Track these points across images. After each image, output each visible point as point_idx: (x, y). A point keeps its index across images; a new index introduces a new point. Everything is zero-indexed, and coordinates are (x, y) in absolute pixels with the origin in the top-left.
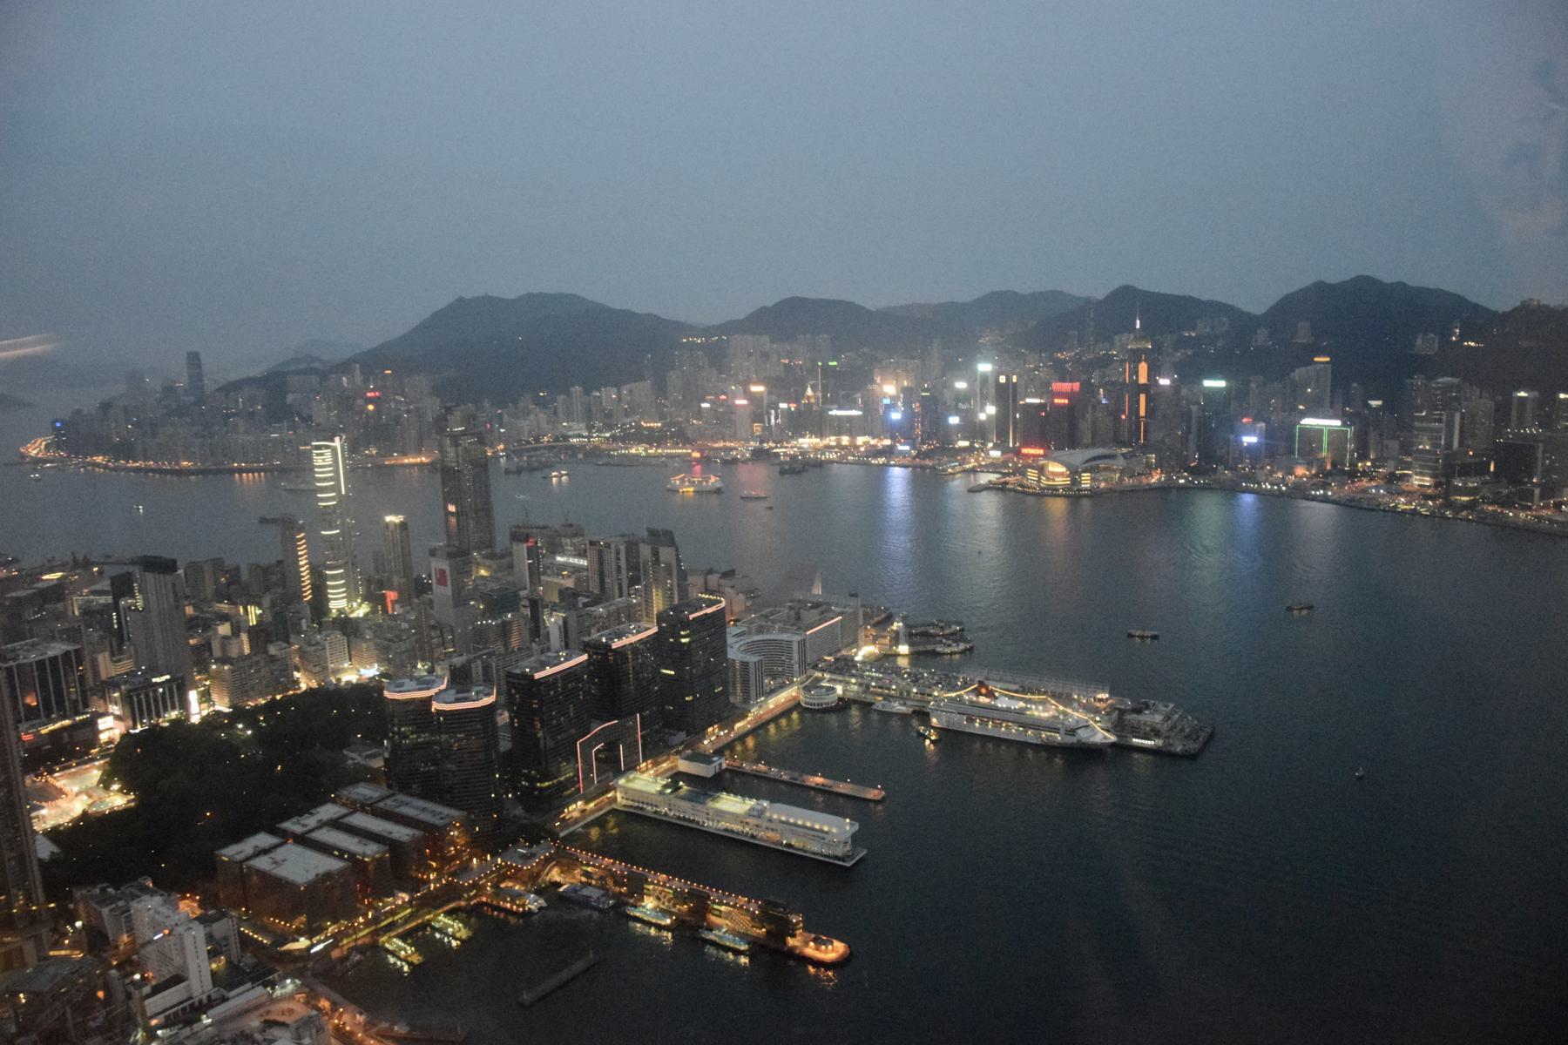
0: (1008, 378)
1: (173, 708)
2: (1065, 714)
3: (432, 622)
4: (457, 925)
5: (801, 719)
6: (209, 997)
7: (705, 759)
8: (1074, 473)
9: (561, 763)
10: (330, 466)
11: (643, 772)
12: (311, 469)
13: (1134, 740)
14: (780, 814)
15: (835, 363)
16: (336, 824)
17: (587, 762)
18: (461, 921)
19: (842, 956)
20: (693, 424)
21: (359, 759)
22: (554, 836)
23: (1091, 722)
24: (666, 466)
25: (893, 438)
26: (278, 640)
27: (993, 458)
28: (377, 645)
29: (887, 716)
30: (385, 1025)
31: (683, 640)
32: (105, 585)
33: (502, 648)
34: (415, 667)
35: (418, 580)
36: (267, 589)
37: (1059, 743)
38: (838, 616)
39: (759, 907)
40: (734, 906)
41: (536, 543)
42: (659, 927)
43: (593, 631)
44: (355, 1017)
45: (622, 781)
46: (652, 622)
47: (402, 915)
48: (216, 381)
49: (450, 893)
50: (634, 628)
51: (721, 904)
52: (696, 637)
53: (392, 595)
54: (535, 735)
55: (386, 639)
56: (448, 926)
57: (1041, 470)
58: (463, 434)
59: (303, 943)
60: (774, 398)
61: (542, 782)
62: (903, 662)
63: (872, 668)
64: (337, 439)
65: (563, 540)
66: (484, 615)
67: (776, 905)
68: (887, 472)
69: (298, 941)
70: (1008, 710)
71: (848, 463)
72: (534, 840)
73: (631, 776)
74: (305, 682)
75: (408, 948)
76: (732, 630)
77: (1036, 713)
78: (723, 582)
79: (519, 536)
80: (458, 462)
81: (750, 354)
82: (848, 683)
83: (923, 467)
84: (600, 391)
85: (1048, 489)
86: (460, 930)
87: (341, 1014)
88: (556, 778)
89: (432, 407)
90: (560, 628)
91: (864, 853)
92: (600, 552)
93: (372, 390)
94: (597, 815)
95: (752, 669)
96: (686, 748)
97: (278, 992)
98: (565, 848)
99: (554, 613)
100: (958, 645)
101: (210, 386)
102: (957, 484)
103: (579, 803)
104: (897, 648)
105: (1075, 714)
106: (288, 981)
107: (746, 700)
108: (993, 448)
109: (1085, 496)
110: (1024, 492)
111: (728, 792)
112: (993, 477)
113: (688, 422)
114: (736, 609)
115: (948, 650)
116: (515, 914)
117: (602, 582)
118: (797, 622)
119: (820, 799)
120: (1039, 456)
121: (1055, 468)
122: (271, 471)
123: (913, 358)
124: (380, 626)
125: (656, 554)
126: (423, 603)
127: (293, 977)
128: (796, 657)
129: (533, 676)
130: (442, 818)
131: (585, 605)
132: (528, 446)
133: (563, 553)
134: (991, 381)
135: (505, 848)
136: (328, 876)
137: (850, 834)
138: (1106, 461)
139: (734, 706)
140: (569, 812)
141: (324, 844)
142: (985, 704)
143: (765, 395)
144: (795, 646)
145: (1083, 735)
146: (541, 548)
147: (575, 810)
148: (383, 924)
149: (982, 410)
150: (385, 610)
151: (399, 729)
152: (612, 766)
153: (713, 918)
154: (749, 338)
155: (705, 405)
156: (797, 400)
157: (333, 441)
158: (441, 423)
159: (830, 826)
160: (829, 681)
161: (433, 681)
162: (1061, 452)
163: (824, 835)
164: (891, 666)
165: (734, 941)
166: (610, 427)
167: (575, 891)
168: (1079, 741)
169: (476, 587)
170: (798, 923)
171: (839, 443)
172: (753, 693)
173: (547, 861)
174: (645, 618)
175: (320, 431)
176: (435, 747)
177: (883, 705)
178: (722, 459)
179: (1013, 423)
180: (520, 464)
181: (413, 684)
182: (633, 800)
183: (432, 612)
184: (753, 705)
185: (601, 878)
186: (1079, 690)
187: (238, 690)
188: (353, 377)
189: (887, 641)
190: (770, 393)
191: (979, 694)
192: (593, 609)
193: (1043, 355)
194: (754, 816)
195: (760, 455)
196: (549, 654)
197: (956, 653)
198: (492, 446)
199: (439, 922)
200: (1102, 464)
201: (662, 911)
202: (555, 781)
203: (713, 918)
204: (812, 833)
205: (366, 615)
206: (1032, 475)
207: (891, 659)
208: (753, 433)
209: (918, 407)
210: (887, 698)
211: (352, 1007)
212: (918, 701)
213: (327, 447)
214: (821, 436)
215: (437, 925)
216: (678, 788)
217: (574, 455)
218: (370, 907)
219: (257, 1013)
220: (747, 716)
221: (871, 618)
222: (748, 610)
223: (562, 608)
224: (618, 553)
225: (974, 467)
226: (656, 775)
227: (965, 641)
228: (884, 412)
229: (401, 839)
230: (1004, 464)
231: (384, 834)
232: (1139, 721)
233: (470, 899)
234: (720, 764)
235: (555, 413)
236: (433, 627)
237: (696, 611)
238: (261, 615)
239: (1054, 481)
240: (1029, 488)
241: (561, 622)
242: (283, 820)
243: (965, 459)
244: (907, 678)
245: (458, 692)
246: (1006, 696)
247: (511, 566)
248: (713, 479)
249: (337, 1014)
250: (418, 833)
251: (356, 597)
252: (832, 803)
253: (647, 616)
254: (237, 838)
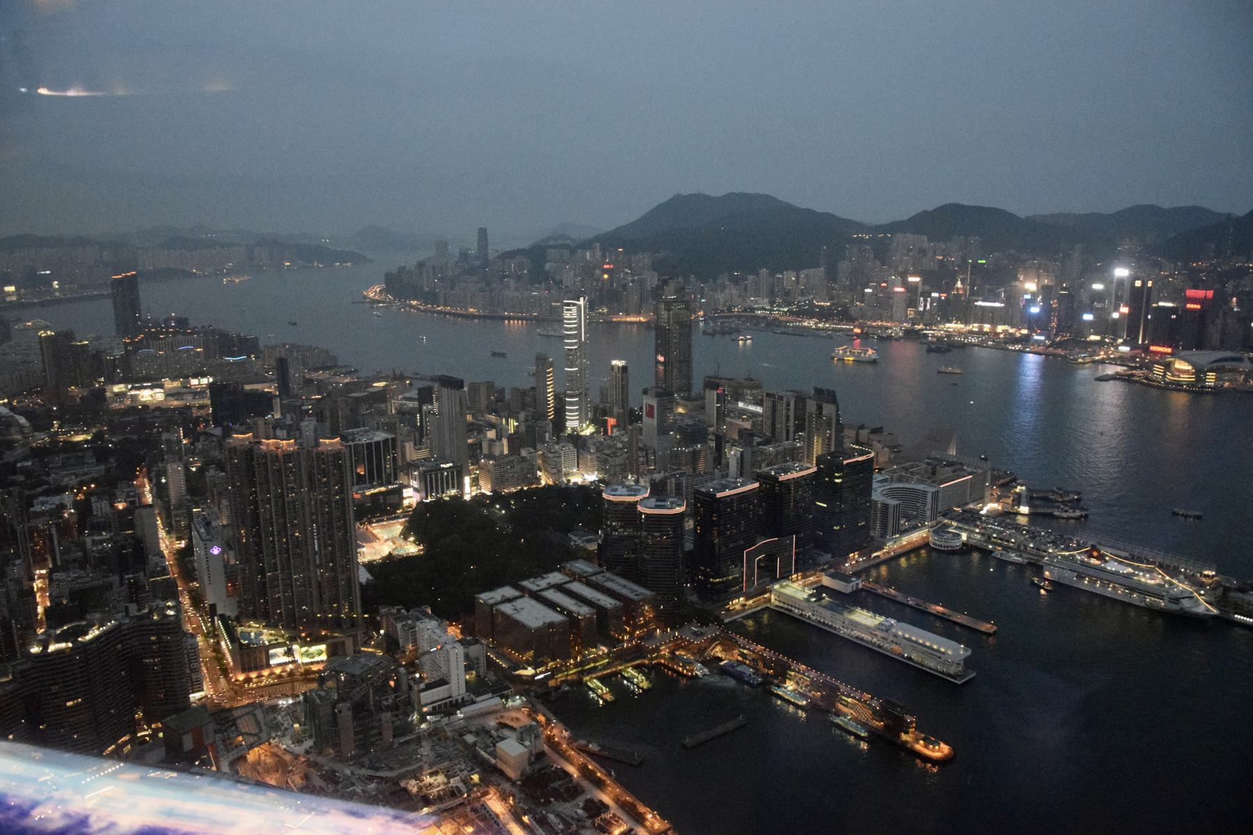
0: (1144, 283)
1: (453, 488)
2: (1171, 584)
3: (641, 445)
4: (641, 677)
5: (929, 556)
6: (463, 699)
7: (845, 578)
8: (1199, 372)
9: (730, 565)
10: (575, 319)
11: (794, 582)
12: (561, 320)
13: (1236, 616)
14: (904, 631)
15: (984, 261)
16: (560, 588)
17: (750, 568)
18: (644, 674)
19: (946, 756)
20: (857, 305)
21: (579, 542)
22: (720, 622)
23: (1195, 594)
24: (831, 338)
25: (1030, 329)
26: (528, 446)
27: (1123, 353)
28: (598, 457)
29: (1002, 564)
30: (583, 742)
31: (837, 481)
32: (414, 393)
33: (692, 470)
34: (626, 477)
35: (632, 411)
36: (523, 409)
37: (1161, 608)
38: (969, 475)
39: (880, 704)
40: (859, 700)
41: (724, 391)
42: (797, 707)
43: (763, 465)
44: (562, 732)
45: (776, 587)
46: (812, 463)
47: (602, 663)
48: (497, 251)
49: (638, 652)
50: (798, 467)
51: (849, 696)
52: (847, 479)
53: (612, 421)
54: (712, 542)
55: (605, 454)
56: (634, 677)
57: (1168, 366)
58: (675, 301)
59: (530, 671)
60: (927, 288)
61: (714, 578)
62: (1022, 520)
63: (995, 522)
64: (582, 299)
65: (745, 390)
66: (679, 444)
67: (895, 706)
68: (1022, 357)
69: (526, 669)
70: (1116, 573)
71: (988, 347)
72: (704, 622)
73: (784, 584)
74: (545, 480)
75: (604, 688)
76: (877, 477)
77: (1143, 580)
78: (871, 436)
79: (711, 384)
80: (668, 323)
81: (909, 250)
82: (973, 532)
83: (1055, 356)
84: (782, 273)
85: (1173, 384)
86: (642, 682)
87: (553, 728)
88: (724, 576)
89: (652, 280)
90: (737, 459)
91: (974, 674)
92: (774, 402)
93: (608, 263)
94: (754, 610)
95: (891, 510)
96: (831, 567)
97: (510, 703)
98: (727, 632)
99: (734, 448)
100: (1074, 512)
101: (492, 255)
102: (1084, 373)
103: (741, 599)
104: (1019, 507)
105: (1181, 585)
106: (518, 697)
107: (883, 535)
108: (1122, 344)
109: (1208, 393)
110: (1149, 384)
111: (862, 608)
112: (1120, 369)
113: (852, 302)
114: (882, 459)
115: (1065, 515)
116: (686, 676)
117: (773, 424)
118: (932, 475)
119: (938, 624)
120: (1167, 354)
121: (1180, 365)
122: (531, 320)
123: (1055, 260)
124: (601, 443)
125: (820, 408)
126: (636, 429)
127: (521, 695)
128: (929, 505)
129: (715, 495)
130: (637, 595)
131: (759, 444)
132: (723, 314)
133: (743, 401)
134: (1127, 285)
135: (682, 625)
136: (551, 625)
137: (963, 658)
138: (1234, 364)
139: (872, 538)
140: (733, 605)
141: (548, 600)
142: (1097, 565)
143: (920, 283)
144: (929, 496)
145: (1186, 604)
146: (727, 396)
147: (736, 604)
148: (587, 667)
149: (1116, 309)
150: (606, 432)
151: (611, 523)
152: (771, 573)
153: (841, 707)
154: (910, 236)
155: (868, 290)
156: (947, 291)
157: (579, 300)
158: (657, 293)
159: (946, 648)
160: (956, 528)
161: (639, 490)
162: (1190, 352)
163: (939, 655)
164: (1011, 522)
165: (856, 728)
166: (788, 304)
167: (733, 667)
168: (1182, 609)
169: (675, 421)
170: (911, 722)
171: (981, 328)
172: (890, 532)
173: (714, 639)
174: (806, 459)
175: (567, 292)
176: (637, 540)
177: (1002, 554)
178: (879, 336)
179: (1144, 325)
180: (715, 328)
181: (625, 491)
182: (784, 603)
183: (642, 437)
184: (890, 540)
185: (753, 660)
186: (1186, 564)
187: (499, 480)
188: (594, 253)
189: (1010, 501)
190: (924, 282)
191: (1091, 556)
192: (764, 447)
193: (1179, 264)
194: (882, 630)
195: (911, 335)
196: (728, 479)
197: (1071, 518)
198: (695, 312)
199: (628, 672)
200: (1228, 365)
201: (799, 693)
202: (725, 579)
203: (841, 707)
204: (930, 651)
205: (592, 434)
206: (1158, 370)
207: (1011, 516)
208: (907, 316)
209: (1056, 303)
210: (1006, 548)
211: (560, 725)
212: (1033, 555)
213: (574, 305)
214: (966, 323)
215: (626, 675)
216: (820, 599)
217: (757, 324)
218: (579, 652)
219: (494, 716)
220: (883, 549)
221: (999, 477)
222: (891, 462)
223: (740, 444)
224: (788, 405)
225: (1103, 359)
226: (805, 586)
227: (1082, 509)
228: (1023, 306)
229: (606, 606)
230: (1133, 359)
231: (593, 600)
232: (1243, 600)
233: (652, 659)
234: (857, 584)
235: (745, 290)
236: (641, 449)
237: (850, 458)
238: (517, 426)
239: (1179, 377)
240: (1154, 381)
241: (739, 455)
242: (523, 580)
243: (1095, 351)
244: (1025, 534)
245: (657, 501)
246: (1116, 561)
247: (703, 408)
248: (870, 352)
249: (550, 728)
250: (618, 603)
251: (586, 420)
252: (948, 629)
253: (808, 458)
254: (490, 587)
